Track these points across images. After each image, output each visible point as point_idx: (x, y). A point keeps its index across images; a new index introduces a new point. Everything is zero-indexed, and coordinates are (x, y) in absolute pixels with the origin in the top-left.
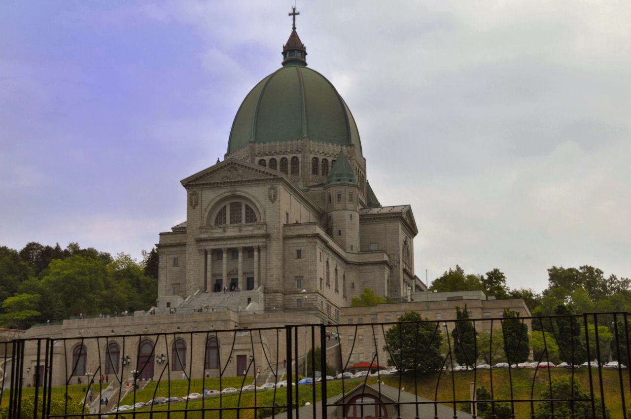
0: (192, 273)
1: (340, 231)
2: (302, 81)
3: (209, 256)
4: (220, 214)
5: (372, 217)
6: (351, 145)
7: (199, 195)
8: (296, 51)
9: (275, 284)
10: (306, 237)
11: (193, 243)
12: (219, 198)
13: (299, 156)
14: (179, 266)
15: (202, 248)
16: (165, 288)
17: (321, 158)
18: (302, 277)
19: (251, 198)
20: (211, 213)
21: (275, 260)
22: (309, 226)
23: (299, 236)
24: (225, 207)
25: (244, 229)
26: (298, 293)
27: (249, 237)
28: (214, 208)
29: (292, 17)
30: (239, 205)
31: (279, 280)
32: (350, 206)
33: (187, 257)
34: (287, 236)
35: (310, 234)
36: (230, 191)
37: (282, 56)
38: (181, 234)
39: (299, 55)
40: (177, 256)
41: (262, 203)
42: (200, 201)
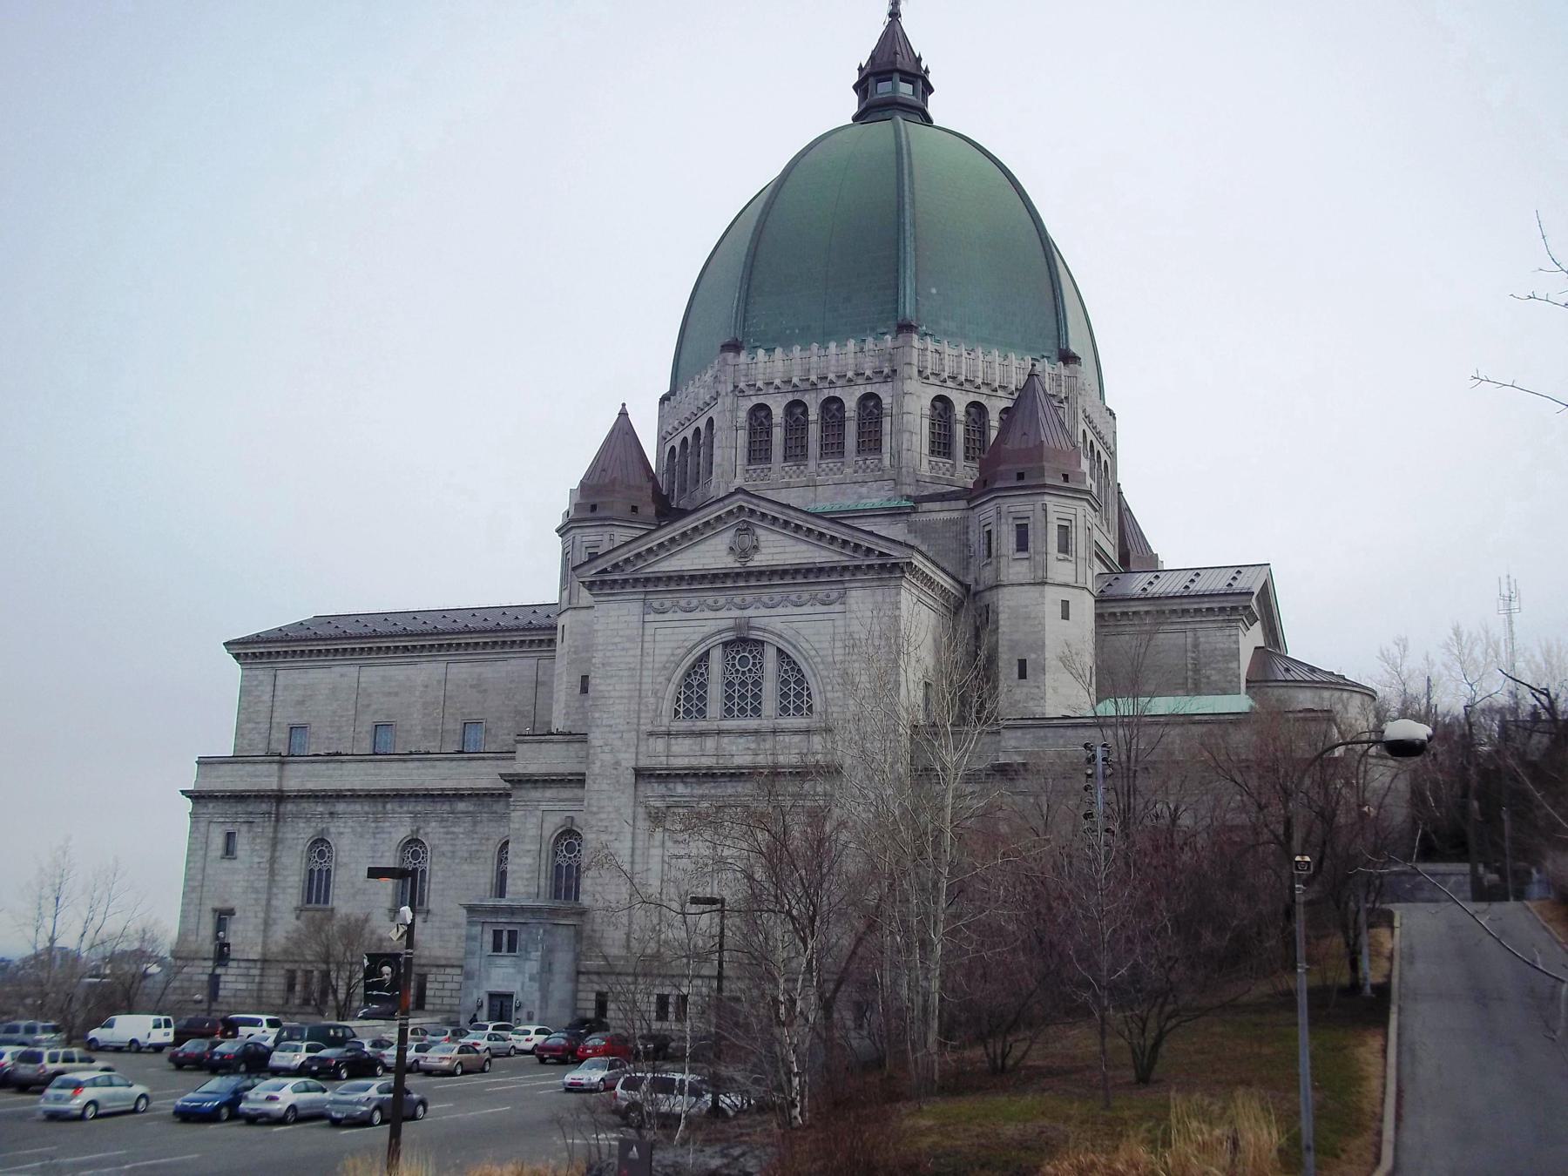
1: (1022, 664)
2: (904, 143)
6: (1068, 358)
8: (896, 77)
13: (885, 393)
17: (960, 402)
32: (1060, 570)
37: (855, 98)
39: (905, 89)
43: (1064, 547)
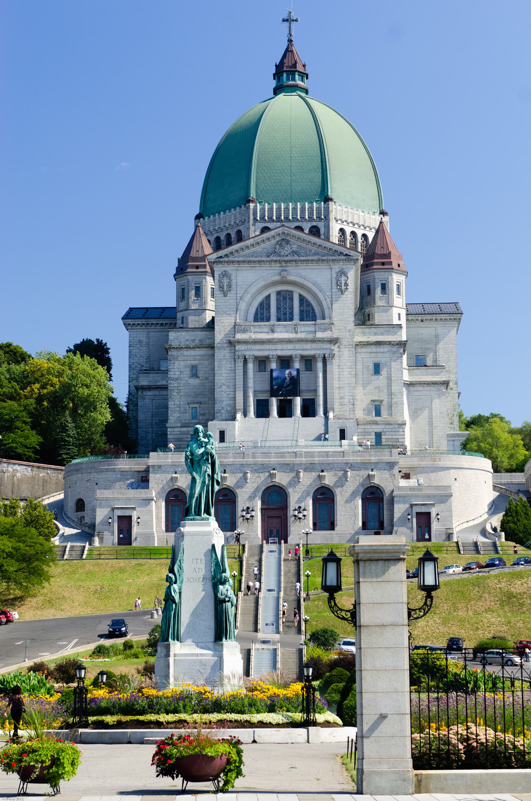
0: (224, 388)
3: (250, 366)
4: (261, 304)
5: (420, 318)
7: (233, 278)
9: (348, 410)
10: (388, 344)
11: (225, 345)
12: (263, 283)
14: (199, 377)
15: (240, 353)
16: (178, 409)
17: (348, 230)
18: (381, 401)
19: (310, 285)
20: (249, 305)
21: (348, 376)
22: (391, 329)
23: (378, 343)
24: (268, 297)
25: (303, 329)
26: (376, 423)
27: (311, 341)
28: (254, 297)
29: (286, 24)
30: (291, 293)
31: (353, 405)
33: (216, 366)
34: (360, 342)
35: (394, 342)
36: (280, 274)
40: (196, 362)
42: (234, 286)
43: (399, 292)
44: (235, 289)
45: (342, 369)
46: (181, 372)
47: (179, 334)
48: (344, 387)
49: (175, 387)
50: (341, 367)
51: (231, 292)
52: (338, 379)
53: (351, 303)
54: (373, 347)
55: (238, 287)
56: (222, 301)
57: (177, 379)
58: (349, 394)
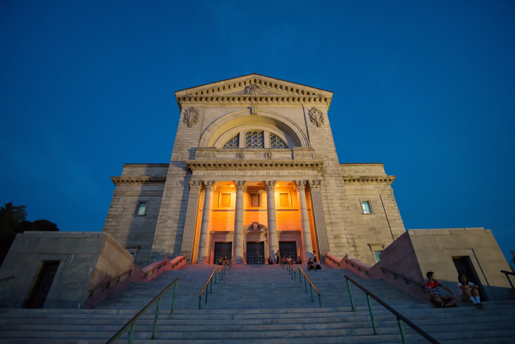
0: (170, 223)
7: (200, 113)
23: (364, 179)
31: (354, 246)
33: (164, 195)
38: (160, 167)
41: (301, 127)
42: (200, 119)
44: (202, 122)
45: (331, 200)
46: (124, 209)
47: (135, 169)
48: (337, 223)
49: (112, 226)
50: (329, 198)
51: (197, 124)
52: (327, 213)
53: (328, 135)
54: (356, 183)
55: (204, 120)
56: (185, 131)
57: (117, 217)
58: (346, 232)
